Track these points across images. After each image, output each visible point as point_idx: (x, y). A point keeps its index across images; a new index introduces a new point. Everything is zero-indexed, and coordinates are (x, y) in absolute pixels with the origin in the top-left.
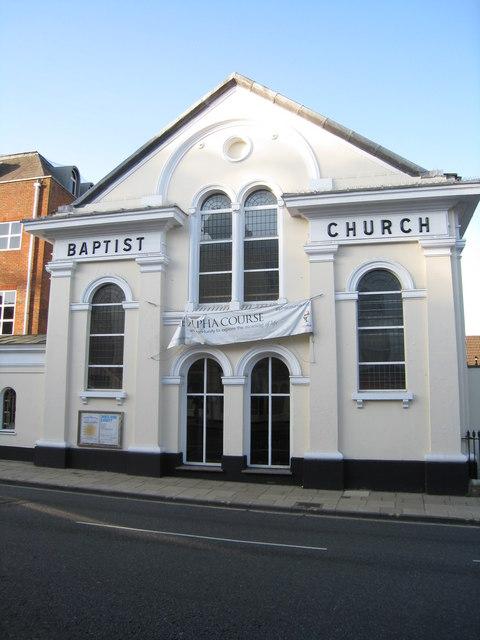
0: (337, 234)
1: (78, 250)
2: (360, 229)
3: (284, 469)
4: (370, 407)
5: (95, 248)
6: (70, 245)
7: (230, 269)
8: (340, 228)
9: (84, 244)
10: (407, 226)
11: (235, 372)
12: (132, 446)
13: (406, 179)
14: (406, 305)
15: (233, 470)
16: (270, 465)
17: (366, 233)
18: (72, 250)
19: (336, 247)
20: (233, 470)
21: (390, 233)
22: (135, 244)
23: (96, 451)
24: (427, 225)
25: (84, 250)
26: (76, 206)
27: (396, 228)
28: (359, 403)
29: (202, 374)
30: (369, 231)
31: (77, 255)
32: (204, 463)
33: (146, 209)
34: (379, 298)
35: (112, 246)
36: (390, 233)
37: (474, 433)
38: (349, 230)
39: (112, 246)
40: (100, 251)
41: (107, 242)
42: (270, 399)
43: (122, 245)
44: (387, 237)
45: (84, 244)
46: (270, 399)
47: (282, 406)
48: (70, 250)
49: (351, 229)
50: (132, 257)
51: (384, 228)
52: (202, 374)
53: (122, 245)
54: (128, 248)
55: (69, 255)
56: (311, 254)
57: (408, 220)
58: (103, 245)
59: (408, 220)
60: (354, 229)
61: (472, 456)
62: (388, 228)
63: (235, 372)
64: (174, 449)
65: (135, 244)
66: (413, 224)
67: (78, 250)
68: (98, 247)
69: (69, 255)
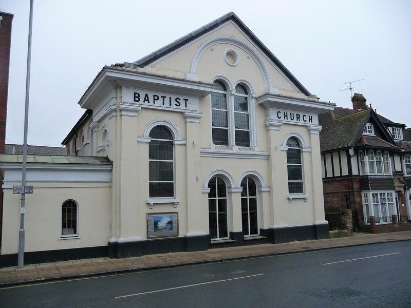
1: (142, 98)
3: (257, 236)
5: (154, 99)
6: (135, 94)
8: (282, 115)
9: (147, 95)
13: (303, 96)
15: (238, 239)
16: (250, 235)
18: (137, 97)
20: (238, 239)
22: (182, 102)
23: (169, 240)
24: (311, 119)
25: (147, 99)
27: (301, 118)
29: (218, 186)
32: (218, 238)
35: (167, 101)
38: (285, 116)
39: (167, 101)
40: (159, 103)
41: (164, 97)
42: (215, 198)
45: (147, 95)
46: (215, 198)
48: (135, 97)
49: (286, 116)
51: (297, 118)
53: (174, 102)
54: (178, 104)
55: (135, 101)
56: (198, 118)
58: (161, 99)
60: (287, 116)
65: (182, 102)
66: (307, 118)
67: (142, 98)
68: (158, 99)
69: (135, 101)
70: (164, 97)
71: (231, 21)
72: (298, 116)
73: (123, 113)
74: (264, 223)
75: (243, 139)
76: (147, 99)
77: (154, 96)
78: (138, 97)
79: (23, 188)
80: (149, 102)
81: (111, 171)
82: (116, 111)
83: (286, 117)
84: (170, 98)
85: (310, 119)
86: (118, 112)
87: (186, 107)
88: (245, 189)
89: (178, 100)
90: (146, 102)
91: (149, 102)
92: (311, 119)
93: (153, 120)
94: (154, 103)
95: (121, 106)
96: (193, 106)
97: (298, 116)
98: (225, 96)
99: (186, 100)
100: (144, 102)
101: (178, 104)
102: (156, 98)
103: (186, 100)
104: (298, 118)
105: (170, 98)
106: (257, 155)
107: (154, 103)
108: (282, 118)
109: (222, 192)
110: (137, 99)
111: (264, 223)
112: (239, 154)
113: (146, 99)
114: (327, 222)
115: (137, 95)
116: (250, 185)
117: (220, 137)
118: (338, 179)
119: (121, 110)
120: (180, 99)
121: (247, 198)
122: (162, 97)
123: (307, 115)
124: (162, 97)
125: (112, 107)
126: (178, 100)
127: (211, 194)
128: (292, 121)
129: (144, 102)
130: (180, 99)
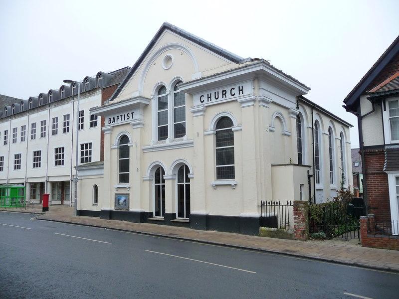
2: (213, 97)
4: (219, 190)
7: (185, 120)
8: (205, 98)
9: (114, 118)
11: (169, 172)
12: (134, 208)
13: (234, 66)
14: (235, 135)
16: (185, 218)
17: (216, 99)
20: (169, 219)
24: (242, 90)
26: (111, 100)
27: (228, 94)
28: (214, 187)
29: (158, 173)
32: (161, 217)
33: (129, 100)
34: (224, 131)
35: (123, 117)
37: (264, 202)
41: (121, 116)
43: (126, 117)
44: (225, 100)
45: (114, 118)
47: (188, 187)
49: (209, 98)
50: (128, 122)
51: (223, 95)
52: (158, 173)
53: (126, 117)
57: (234, 89)
58: (120, 117)
59: (234, 89)
60: (210, 97)
61: (273, 213)
63: (169, 172)
64: (147, 210)
65: (130, 115)
66: (236, 91)
71: (166, 30)
72: (224, 93)
74: (196, 209)
75: (180, 131)
93: (214, 115)
96: (137, 115)
99: (132, 113)
103: (132, 113)
106: (184, 144)
108: (206, 101)
111: (196, 209)
112: (169, 146)
116: (183, 171)
117: (163, 133)
128: (216, 100)
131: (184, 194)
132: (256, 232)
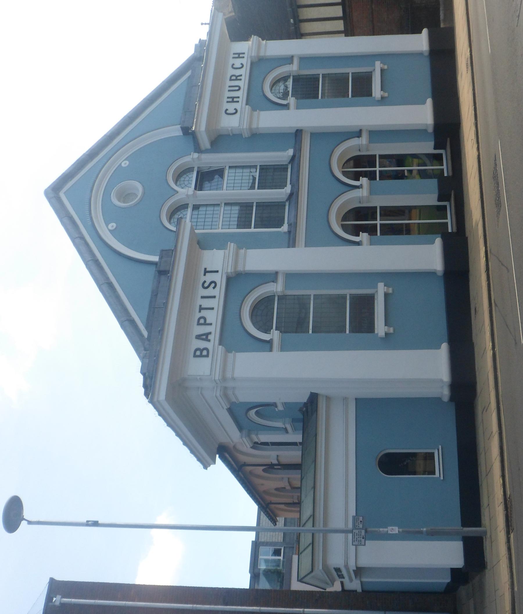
0: (235, 109)
1: (202, 344)
5: (205, 324)
6: (195, 356)
8: (231, 108)
9: (199, 337)
10: (238, 65)
15: (452, 187)
18: (201, 353)
19: (247, 106)
21: (241, 75)
22: (209, 278)
24: (239, 54)
25: (205, 337)
27: (237, 72)
30: (237, 88)
31: (209, 345)
35: (206, 303)
36: (241, 75)
38: (233, 101)
39: (206, 303)
41: (201, 309)
45: (199, 337)
48: (201, 356)
49: (233, 100)
51: (236, 79)
54: (213, 285)
55: (207, 356)
58: (204, 313)
60: (233, 98)
62: (237, 77)
65: (209, 278)
66: (238, 63)
67: (202, 344)
69: (207, 356)
70: (201, 309)
72: (234, 78)
73: (229, 375)
76: (205, 337)
77: (199, 324)
78: (202, 350)
79: (356, 531)
80: (210, 333)
81: (328, 398)
82: (226, 388)
83: (235, 100)
84: (203, 297)
85: (239, 57)
86: (230, 384)
87: (217, 272)
88: (365, 174)
89: (206, 285)
90: (210, 337)
91: (210, 333)
92: (239, 55)
94: (211, 324)
95: (217, 378)
97: (234, 78)
98: (196, 207)
99: (206, 272)
100: (209, 341)
101: (213, 285)
102: (202, 321)
103: (206, 272)
104: (237, 78)
105: (203, 297)
107: (211, 324)
108: (238, 106)
109: (370, 160)
110: (205, 353)
113: (204, 337)
114: (425, 31)
115: (198, 353)
118: (348, 10)
119: (224, 379)
120: (205, 282)
121: (380, 171)
122: (200, 312)
123: (231, 61)
124: (200, 312)
125: (218, 395)
126: (206, 285)
127: (371, 230)
129: (209, 341)
130: (205, 282)
131: (397, 167)
132: (451, 32)
